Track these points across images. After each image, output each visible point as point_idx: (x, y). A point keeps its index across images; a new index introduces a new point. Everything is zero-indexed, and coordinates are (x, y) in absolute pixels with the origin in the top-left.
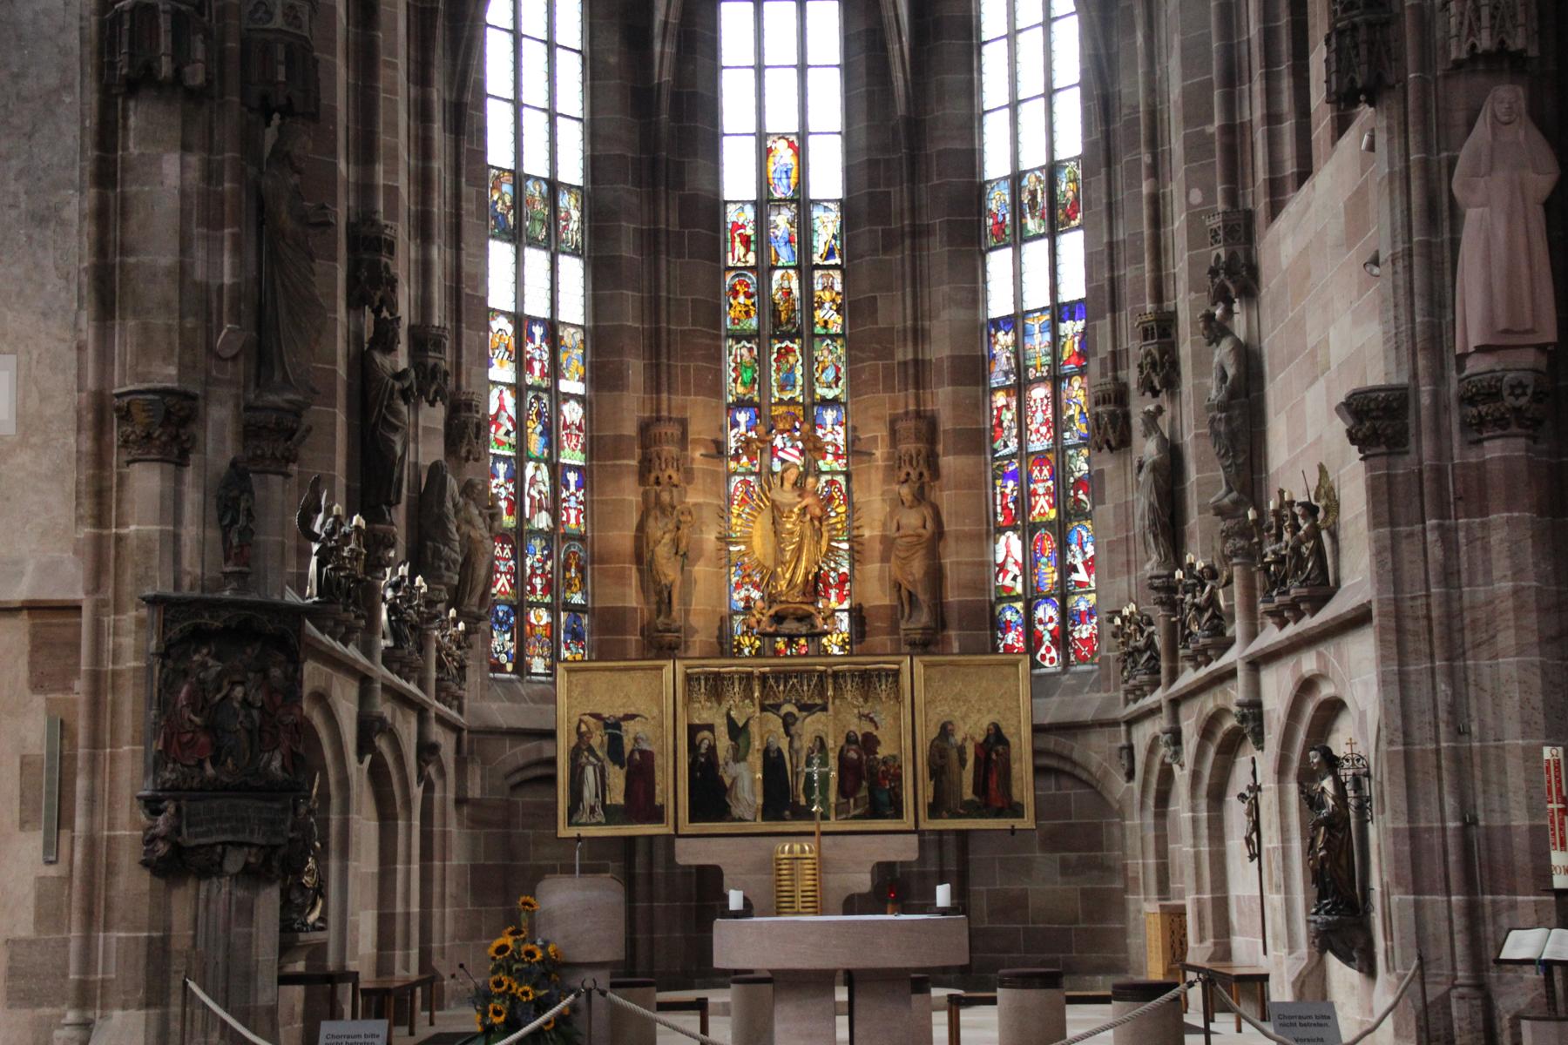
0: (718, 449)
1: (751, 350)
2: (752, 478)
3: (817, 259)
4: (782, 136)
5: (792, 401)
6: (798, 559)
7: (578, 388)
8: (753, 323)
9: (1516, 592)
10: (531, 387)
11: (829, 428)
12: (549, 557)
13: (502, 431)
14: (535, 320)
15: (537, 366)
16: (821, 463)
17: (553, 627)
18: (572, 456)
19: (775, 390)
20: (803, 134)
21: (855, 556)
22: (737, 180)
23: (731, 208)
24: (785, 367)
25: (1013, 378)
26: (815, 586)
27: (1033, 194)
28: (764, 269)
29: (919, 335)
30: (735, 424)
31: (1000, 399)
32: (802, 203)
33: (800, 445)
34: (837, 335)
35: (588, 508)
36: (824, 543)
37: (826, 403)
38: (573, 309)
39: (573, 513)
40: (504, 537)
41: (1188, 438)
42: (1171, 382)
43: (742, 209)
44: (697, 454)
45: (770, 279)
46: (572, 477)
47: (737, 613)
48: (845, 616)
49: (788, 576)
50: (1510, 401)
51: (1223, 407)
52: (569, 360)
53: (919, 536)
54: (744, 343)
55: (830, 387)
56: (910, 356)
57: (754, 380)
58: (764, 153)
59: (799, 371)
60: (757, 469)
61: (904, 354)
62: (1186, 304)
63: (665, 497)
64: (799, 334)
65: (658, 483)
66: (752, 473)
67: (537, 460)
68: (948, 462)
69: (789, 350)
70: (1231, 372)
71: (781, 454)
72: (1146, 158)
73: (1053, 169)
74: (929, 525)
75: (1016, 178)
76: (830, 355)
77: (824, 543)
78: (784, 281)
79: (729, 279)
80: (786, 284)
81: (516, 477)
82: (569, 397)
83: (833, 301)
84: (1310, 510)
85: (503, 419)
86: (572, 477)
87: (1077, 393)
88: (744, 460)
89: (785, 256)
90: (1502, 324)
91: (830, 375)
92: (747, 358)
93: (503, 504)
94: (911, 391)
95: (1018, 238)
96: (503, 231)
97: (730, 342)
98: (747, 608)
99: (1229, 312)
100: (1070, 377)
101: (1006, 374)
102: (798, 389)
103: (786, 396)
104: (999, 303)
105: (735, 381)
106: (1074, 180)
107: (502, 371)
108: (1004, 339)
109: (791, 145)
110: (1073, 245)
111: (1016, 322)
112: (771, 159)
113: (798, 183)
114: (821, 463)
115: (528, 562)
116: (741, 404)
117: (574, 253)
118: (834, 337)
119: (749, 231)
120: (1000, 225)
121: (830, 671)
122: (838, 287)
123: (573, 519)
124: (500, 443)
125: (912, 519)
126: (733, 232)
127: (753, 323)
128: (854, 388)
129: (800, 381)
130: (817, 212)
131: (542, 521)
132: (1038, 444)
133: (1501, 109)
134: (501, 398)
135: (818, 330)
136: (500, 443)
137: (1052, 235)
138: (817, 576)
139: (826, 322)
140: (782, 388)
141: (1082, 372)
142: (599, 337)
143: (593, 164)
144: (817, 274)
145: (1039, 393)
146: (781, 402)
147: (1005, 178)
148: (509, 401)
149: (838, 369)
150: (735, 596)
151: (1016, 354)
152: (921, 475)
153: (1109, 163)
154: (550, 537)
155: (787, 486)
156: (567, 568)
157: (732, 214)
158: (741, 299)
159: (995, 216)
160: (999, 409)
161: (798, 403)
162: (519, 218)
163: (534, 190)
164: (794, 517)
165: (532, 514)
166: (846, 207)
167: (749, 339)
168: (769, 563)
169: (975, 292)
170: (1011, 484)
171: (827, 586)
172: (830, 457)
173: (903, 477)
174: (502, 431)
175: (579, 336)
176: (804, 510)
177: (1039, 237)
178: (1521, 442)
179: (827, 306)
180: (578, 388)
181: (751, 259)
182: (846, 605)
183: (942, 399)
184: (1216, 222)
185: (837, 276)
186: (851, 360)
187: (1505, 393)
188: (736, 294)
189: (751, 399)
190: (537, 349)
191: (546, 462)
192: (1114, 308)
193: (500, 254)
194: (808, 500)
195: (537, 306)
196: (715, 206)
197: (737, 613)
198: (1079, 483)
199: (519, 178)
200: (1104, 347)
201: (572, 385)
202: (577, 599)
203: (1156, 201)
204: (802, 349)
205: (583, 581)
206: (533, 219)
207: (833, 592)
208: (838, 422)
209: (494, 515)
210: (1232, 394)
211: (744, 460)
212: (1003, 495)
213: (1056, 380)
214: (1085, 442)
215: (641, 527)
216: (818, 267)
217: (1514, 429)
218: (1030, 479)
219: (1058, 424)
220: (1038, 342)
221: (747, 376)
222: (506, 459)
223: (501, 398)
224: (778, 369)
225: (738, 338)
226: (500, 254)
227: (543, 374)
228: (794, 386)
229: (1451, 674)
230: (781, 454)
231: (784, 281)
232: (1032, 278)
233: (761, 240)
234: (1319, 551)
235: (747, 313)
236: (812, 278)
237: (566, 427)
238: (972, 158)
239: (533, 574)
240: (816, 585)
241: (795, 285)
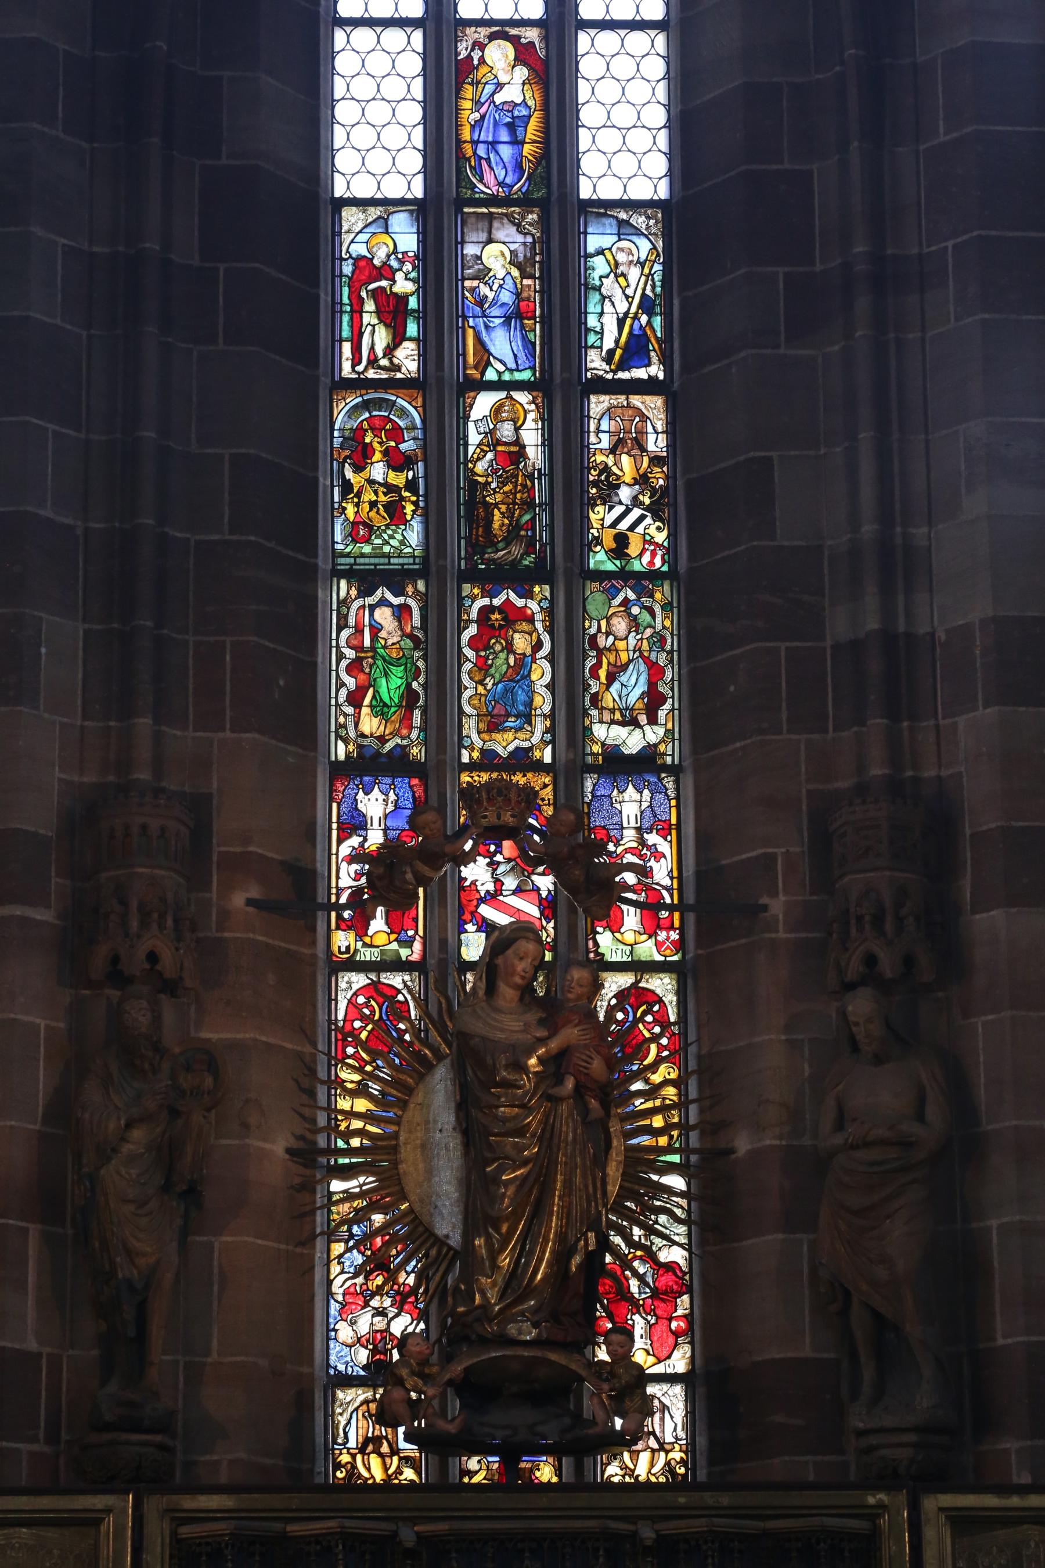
0: (300, 894)
1: (401, 613)
2: (396, 980)
3: (595, 362)
4: (501, 29)
5: (522, 760)
6: (539, 1211)
11: (629, 835)
16: (605, 940)
19: (470, 727)
22: (374, 137)
23: (352, 218)
24: (501, 663)
26: (584, 1294)
29: (898, 566)
30: (356, 824)
33: (545, 883)
34: (653, 575)
36: (614, 1170)
37: (619, 766)
43: (384, 222)
44: (238, 900)
47: (347, 1381)
48: (673, 1399)
49: (505, 1261)
53: (906, 1144)
54: (383, 592)
55: (634, 723)
56: (873, 624)
57: (410, 698)
58: (447, 74)
59: (541, 674)
60: (416, 951)
63: (138, 1013)
64: (541, 573)
65: (117, 976)
66: (398, 965)
69: (513, 616)
71: (485, 910)
74: (934, 1112)
76: (632, 634)
77: (614, 1170)
79: (343, 413)
80: (506, 431)
83: (642, 480)
88: (378, 924)
91: (633, 686)
94: (877, 722)
98: (377, 1372)
102: (540, 726)
103: (505, 744)
105: (355, 699)
109: (524, 54)
112: (468, 91)
113: (543, 158)
114: (605, 940)
116: (371, 765)
118: (644, 582)
121: (647, 1533)
122: (656, 444)
125: (882, 1095)
126: (355, 284)
128: (702, 724)
129: (543, 702)
130: (598, 238)
135: (600, 560)
138: (593, 1261)
139: (622, 540)
146: (488, 760)
150: (345, 1333)
152: (909, 962)
155: (507, 994)
157: (356, 238)
158: (378, 471)
161: (538, 767)
164: (527, 1083)
166: (686, 221)
168: (448, 1226)
172: (631, 919)
173: (854, 968)
176: (557, 1064)
179: (625, 494)
181: (408, 359)
182: (679, 1362)
186: (699, 646)
188: (361, 459)
189: (402, 751)
194: (571, 1034)
197: (347, 1381)
204: (550, 613)
207: (639, 1324)
211: (378, 924)
215: (63, 1108)
221: (390, 686)
224: (483, 667)
225: (367, 580)
228: (527, 718)
230: (485, 910)
233: (440, 302)
235: (395, 514)
236: (584, 417)
240: (591, 1298)
241: (531, 436)
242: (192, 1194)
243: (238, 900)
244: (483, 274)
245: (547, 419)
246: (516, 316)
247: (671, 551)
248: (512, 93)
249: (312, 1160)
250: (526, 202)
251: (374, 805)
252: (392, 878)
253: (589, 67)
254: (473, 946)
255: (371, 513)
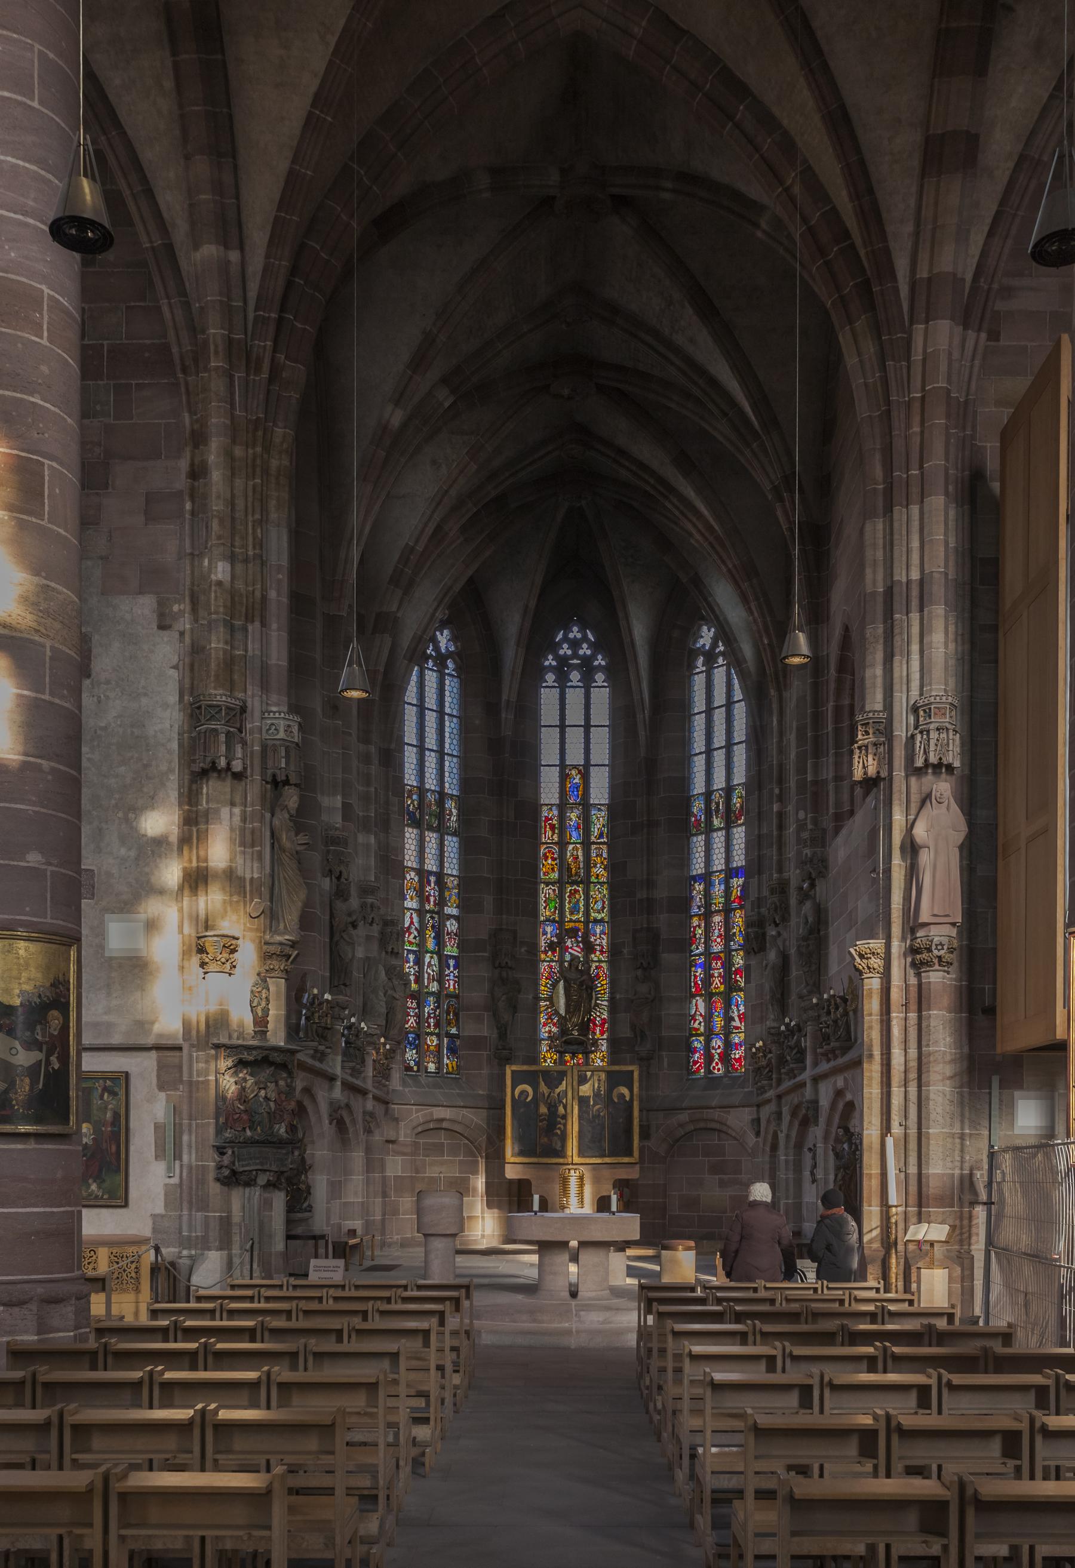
0: (533, 948)
1: (554, 890)
3: (593, 839)
4: (575, 767)
7: (454, 911)
10: (429, 911)
12: (438, 1007)
13: (412, 936)
14: (430, 873)
15: (432, 899)
17: (439, 1046)
18: (451, 950)
20: (587, 764)
21: (613, 1008)
22: (549, 792)
23: (545, 808)
24: (574, 900)
25: (703, 910)
27: (718, 804)
28: (562, 844)
29: (650, 884)
30: (545, 933)
31: (695, 921)
32: (586, 806)
35: (459, 980)
37: (596, 921)
38: (452, 868)
39: (452, 983)
40: (414, 996)
41: (793, 951)
42: (785, 919)
43: (551, 809)
44: (523, 950)
46: (452, 962)
51: (805, 939)
52: (450, 896)
58: (564, 777)
61: (642, 894)
62: (793, 875)
63: (504, 974)
64: (582, 882)
65: (500, 966)
66: (553, 961)
67: (431, 952)
68: (667, 958)
70: (810, 919)
72: (777, 791)
73: (729, 790)
75: (708, 794)
76: (600, 894)
78: (574, 851)
79: (543, 850)
81: (419, 962)
82: (450, 917)
84: (845, 1000)
85: (413, 930)
86: (452, 962)
87: (739, 919)
89: (575, 837)
91: (599, 905)
92: (552, 895)
93: (412, 978)
95: (709, 829)
96: (413, 822)
97: (542, 885)
99: (813, 885)
100: (735, 910)
101: (699, 907)
103: (574, 918)
104: (698, 867)
106: (741, 797)
107: (411, 903)
108: (699, 887)
109: (580, 772)
110: (739, 834)
111: (706, 878)
113: (583, 795)
115: (426, 1010)
117: (454, 834)
120: (698, 822)
122: (605, 855)
123: (451, 985)
124: (411, 943)
126: (545, 822)
127: (555, 876)
131: (434, 987)
132: (717, 948)
134: (411, 918)
135: (593, 879)
136: (411, 943)
137: (728, 828)
140: (572, 913)
141: (741, 908)
142: (466, 882)
143: (466, 783)
144: (593, 847)
145: (717, 919)
146: (571, 921)
147: (702, 794)
148: (416, 919)
149: (604, 903)
151: (705, 896)
153: (760, 788)
154: (438, 995)
156: (448, 1013)
158: (550, 861)
159: (695, 816)
160: (695, 928)
162: (422, 815)
163: (431, 798)
165: (429, 983)
167: (553, 884)
168: (562, 1012)
169: (685, 860)
170: (699, 970)
171: (595, 1025)
174: (412, 936)
175: (456, 882)
177: (720, 829)
180: (454, 911)
181: (556, 838)
183: (662, 920)
184: (805, 835)
185: (604, 847)
186: (612, 897)
188: (546, 859)
190: (431, 889)
191: (436, 953)
192: (760, 873)
193: (411, 835)
194: (585, 977)
195: (431, 865)
196: (535, 808)
198: (738, 972)
199: (422, 790)
200: (753, 895)
201: (451, 910)
202: (454, 1031)
203: (781, 815)
205: (457, 1021)
206: (430, 815)
208: (603, 933)
209: (407, 984)
210: (811, 932)
212: (696, 977)
213: (727, 911)
214: (743, 947)
216: (594, 843)
218: (710, 968)
219: (728, 937)
220: (718, 890)
222: (414, 952)
223: (411, 918)
224: (570, 902)
226: (411, 835)
227: (435, 904)
231: (574, 851)
232: (719, 852)
234: (848, 1025)
235: (553, 869)
237: (448, 934)
238: (684, 782)
239: (429, 1017)
241: (580, 853)
242: (515, 1007)
243: (523, 950)
244: (571, 820)
245: (583, 850)
246: (578, 827)
247: (608, 878)
248: (577, 781)
249: (537, 999)
250: (580, 804)
251: (549, 929)
252: (551, 946)
253: (592, 774)
254: (568, 957)
255: (549, 870)
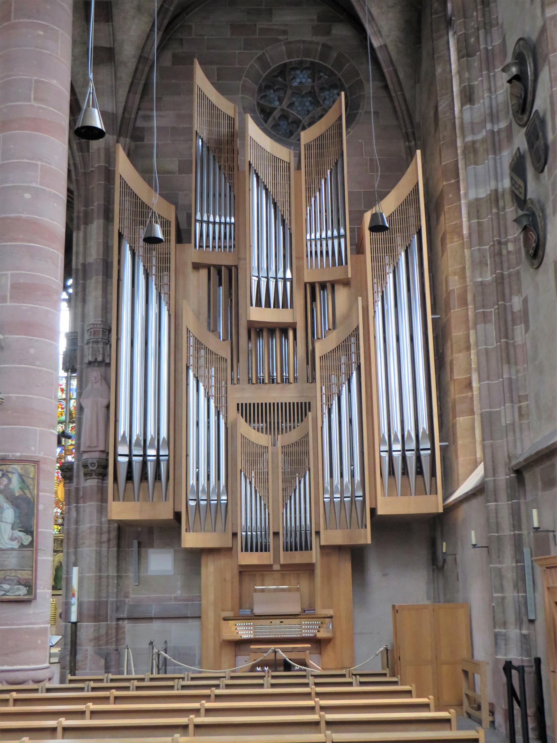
1: (62, 427)
8: (63, 418)
9: (91, 528)
45: (70, 403)
50: (91, 468)
90: (88, 445)
119: (64, 387)
133: (93, 378)
158: (60, 410)
178: (96, 480)
187: (89, 465)
217: (94, 476)
229: (76, 553)
235: (62, 414)
